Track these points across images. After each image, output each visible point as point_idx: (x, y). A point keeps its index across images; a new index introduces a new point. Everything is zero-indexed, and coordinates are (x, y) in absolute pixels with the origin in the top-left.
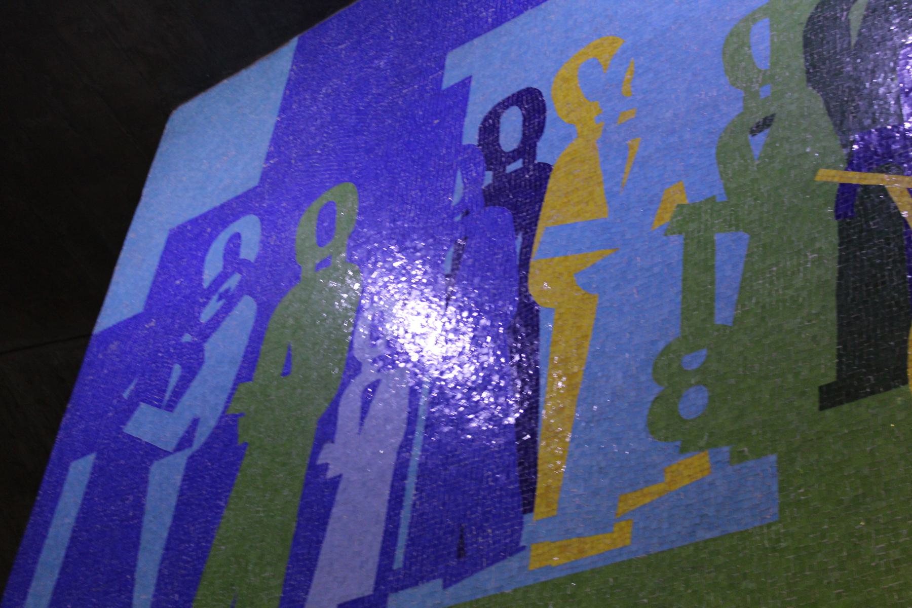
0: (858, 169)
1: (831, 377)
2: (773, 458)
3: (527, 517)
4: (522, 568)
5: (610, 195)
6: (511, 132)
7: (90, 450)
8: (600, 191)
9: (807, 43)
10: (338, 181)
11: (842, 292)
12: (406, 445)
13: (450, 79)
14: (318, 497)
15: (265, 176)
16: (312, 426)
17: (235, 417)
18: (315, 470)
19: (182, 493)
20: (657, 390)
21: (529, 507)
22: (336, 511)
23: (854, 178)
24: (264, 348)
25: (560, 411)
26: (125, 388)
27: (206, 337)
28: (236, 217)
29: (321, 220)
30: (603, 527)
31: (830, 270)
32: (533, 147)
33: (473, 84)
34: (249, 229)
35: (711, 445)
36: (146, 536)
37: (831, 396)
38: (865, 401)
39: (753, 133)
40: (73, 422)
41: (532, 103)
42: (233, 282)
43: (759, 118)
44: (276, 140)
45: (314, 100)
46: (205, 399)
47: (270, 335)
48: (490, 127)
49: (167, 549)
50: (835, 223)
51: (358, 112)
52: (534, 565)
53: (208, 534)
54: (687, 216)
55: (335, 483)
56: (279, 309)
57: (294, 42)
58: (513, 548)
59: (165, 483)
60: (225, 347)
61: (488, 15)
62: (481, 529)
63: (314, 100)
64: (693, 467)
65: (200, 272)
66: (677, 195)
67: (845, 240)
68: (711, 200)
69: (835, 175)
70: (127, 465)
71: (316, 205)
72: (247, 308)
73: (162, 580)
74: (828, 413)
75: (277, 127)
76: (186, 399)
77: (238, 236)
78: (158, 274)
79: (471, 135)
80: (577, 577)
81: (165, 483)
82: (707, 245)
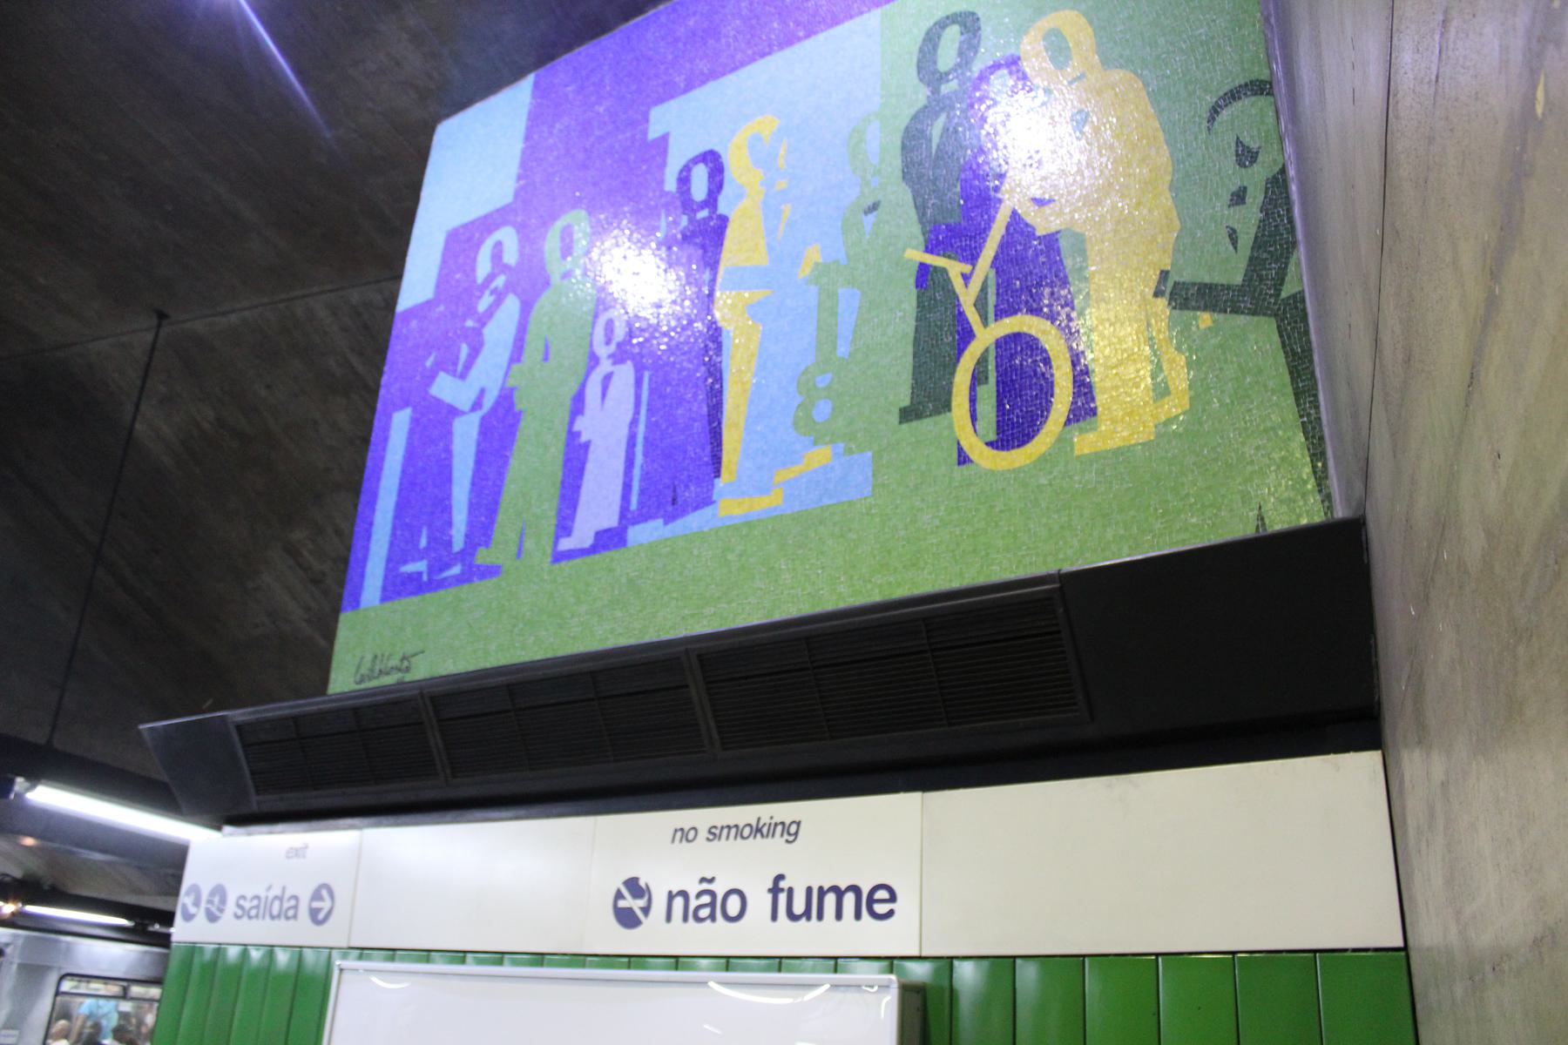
0: (931, 252)
1: (906, 402)
2: (870, 454)
4: (714, 515)
5: (770, 248)
6: (699, 190)
7: (406, 404)
8: (762, 242)
9: (904, 147)
10: (574, 207)
11: (916, 342)
12: (634, 422)
13: (654, 133)
14: (576, 456)
15: (517, 194)
16: (568, 403)
17: (512, 390)
18: (572, 435)
19: (479, 444)
22: (589, 466)
26: (426, 357)
27: (484, 324)
28: (498, 227)
29: (563, 239)
30: (765, 491)
32: (716, 200)
33: (671, 141)
34: (508, 237)
35: (831, 442)
36: (456, 474)
37: (907, 415)
38: (926, 421)
39: (866, 213)
40: (391, 382)
41: (713, 161)
42: (500, 281)
43: (870, 202)
44: (524, 164)
45: (550, 133)
46: (489, 372)
47: (532, 328)
48: (684, 180)
49: (473, 484)
50: (914, 291)
51: (586, 150)
52: (722, 513)
53: (501, 475)
54: (821, 270)
55: (586, 446)
56: (537, 306)
57: (530, 80)
58: (706, 501)
59: (465, 437)
60: (499, 332)
61: (680, 80)
62: (687, 487)
63: (550, 133)
64: (821, 456)
65: (473, 270)
67: (920, 305)
69: (918, 255)
70: (434, 422)
71: (559, 224)
72: (512, 304)
73: (473, 508)
74: (905, 426)
75: (524, 152)
76: (474, 372)
77: (499, 245)
78: (441, 269)
79: (671, 185)
80: (749, 524)
81: (465, 437)
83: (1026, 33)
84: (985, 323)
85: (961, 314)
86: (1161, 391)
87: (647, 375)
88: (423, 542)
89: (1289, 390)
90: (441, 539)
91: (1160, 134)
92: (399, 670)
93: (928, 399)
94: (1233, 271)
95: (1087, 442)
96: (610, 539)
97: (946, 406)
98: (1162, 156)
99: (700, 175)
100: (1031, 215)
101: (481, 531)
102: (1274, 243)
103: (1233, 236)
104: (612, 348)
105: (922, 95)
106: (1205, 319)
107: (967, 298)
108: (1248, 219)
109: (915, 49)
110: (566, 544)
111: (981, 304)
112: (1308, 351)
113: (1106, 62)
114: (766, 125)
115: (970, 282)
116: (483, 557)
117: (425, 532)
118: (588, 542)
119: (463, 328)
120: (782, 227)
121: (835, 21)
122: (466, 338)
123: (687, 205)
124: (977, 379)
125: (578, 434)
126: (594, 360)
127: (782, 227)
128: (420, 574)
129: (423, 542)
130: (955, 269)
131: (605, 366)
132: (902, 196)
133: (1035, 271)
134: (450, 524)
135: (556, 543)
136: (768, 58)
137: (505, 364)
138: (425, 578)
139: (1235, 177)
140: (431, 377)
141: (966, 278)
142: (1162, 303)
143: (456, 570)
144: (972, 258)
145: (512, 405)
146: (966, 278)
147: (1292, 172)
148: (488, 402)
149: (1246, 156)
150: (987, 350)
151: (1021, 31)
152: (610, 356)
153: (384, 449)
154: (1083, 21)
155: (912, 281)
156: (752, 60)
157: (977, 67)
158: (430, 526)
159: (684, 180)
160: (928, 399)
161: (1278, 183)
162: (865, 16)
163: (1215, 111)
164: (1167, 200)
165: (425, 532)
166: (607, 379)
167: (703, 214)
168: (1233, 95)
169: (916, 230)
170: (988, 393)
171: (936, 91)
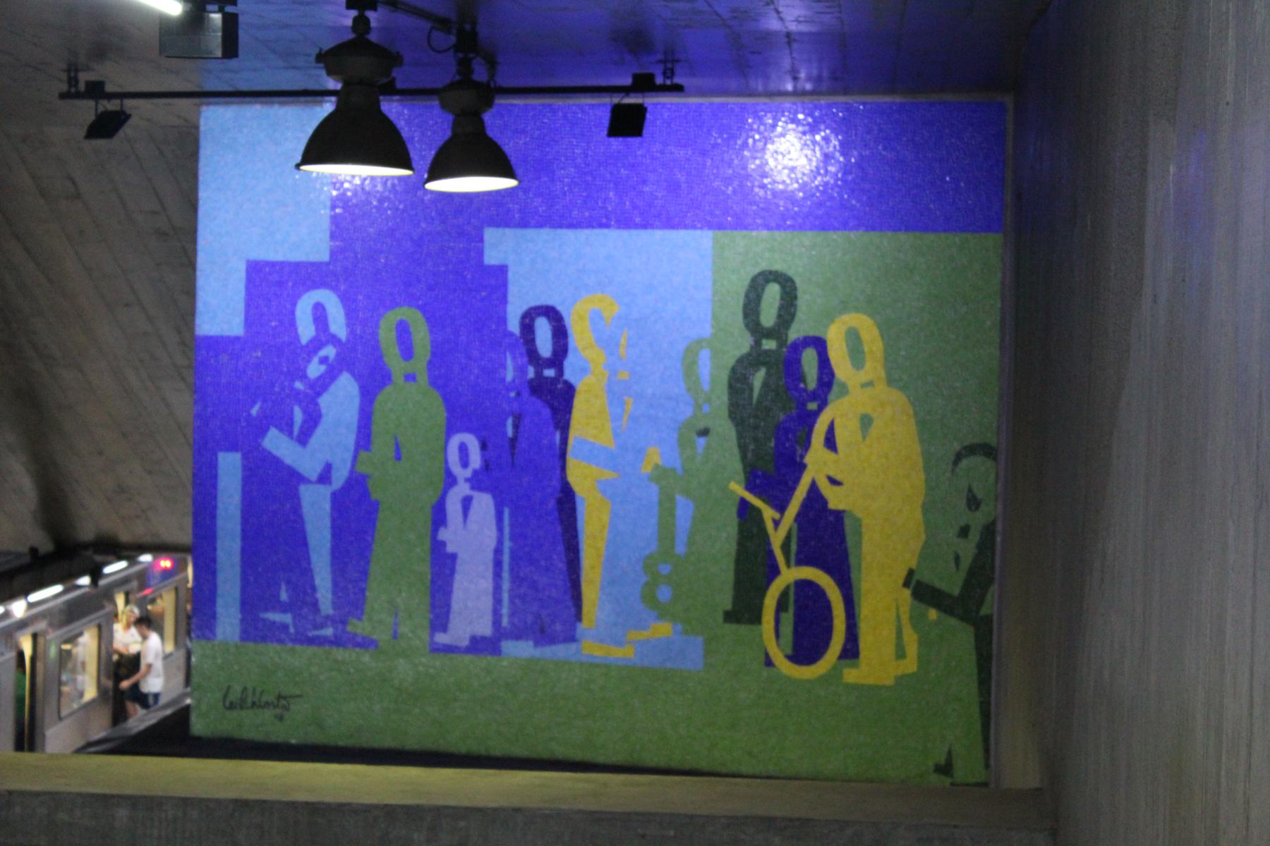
1: (729, 607)
3: (578, 624)
5: (616, 435)
6: (545, 345)
7: (233, 447)
8: (609, 425)
12: (498, 551)
13: (492, 257)
14: (443, 564)
16: (428, 511)
19: (333, 521)
20: (644, 579)
21: (578, 617)
24: (374, 428)
25: (593, 568)
27: (319, 394)
30: (620, 643)
31: (732, 547)
37: (730, 617)
42: (330, 351)
43: (702, 425)
47: (377, 418)
52: (585, 652)
54: (661, 474)
55: (453, 557)
56: (380, 398)
59: (316, 507)
64: (663, 629)
65: (293, 324)
66: (654, 457)
67: (741, 531)
68: (674, 470)
79: (514, 326)
82: (671, 499)
83: (832, 321)
84: (788, 566)
85: (771, 553)
86: (900, 653)
87: (507, 512)
88: (284, 596)
89: (975, 677)
90: (304, 597)
91: (920, 459)
92: (276, 707)
93: (745, 610)
94: (952, 584)
95: (851, 675)
97: (756, 619)
98: (919, 478)
99: (543, 329)
100: (826, 490)
103: (957, 559)
104: (468, 473)
105: (743, 343)
106: (933, 614)
107: (777, 539)
108: (968, 549)
109: (742, 292)
110: (441, 638)
111: (786, 546)
112: (990, 657)
113: (890, 381)
114: (610, 308)
115: (780, 527)
117: (283, 587)
118: (465, 643)
119: (292, 389)
120: (626, 417)
121: (670, 223)
122: (300, 402)
123: (533, 355)
124: (781, 606)
125: (443, 544)
126: (451, 480)
127: (626, 417)
128: (285, 627)
129: (284, 596)
130: (768, 513)
131: (462, 489)
132: (726, 430)
133: (825, 536)
134: (314, 589)
135: (432, 636)
136: (605, 231)
137: (352, 448)
138: (292, 630)
140: (263, 431)
141: (777, 523)
142: (907, 593)
143: (329, 632)
144: (781, 508)
145: (365, 494)
146: (777, 523)
147: (999, 527)
149: (973, 503)
150: (788, 587)
151: (830, 317)
152: (467, 480)
153: (215, 486)
154: (876, 332)
155: (734, 510)
156: (590, 226)
157: (794, 334)
158: (288, 582)
160: (745, 610)
161: (989, 530)
162: (698, 232)
163: (958, 457)
164: (918, 515)
165: (283, 587)
166: (467, 503)
167: (550, 373)
168: (971, 450)
169: (738, 466)
170: (788, 618)
171: (758, 343)
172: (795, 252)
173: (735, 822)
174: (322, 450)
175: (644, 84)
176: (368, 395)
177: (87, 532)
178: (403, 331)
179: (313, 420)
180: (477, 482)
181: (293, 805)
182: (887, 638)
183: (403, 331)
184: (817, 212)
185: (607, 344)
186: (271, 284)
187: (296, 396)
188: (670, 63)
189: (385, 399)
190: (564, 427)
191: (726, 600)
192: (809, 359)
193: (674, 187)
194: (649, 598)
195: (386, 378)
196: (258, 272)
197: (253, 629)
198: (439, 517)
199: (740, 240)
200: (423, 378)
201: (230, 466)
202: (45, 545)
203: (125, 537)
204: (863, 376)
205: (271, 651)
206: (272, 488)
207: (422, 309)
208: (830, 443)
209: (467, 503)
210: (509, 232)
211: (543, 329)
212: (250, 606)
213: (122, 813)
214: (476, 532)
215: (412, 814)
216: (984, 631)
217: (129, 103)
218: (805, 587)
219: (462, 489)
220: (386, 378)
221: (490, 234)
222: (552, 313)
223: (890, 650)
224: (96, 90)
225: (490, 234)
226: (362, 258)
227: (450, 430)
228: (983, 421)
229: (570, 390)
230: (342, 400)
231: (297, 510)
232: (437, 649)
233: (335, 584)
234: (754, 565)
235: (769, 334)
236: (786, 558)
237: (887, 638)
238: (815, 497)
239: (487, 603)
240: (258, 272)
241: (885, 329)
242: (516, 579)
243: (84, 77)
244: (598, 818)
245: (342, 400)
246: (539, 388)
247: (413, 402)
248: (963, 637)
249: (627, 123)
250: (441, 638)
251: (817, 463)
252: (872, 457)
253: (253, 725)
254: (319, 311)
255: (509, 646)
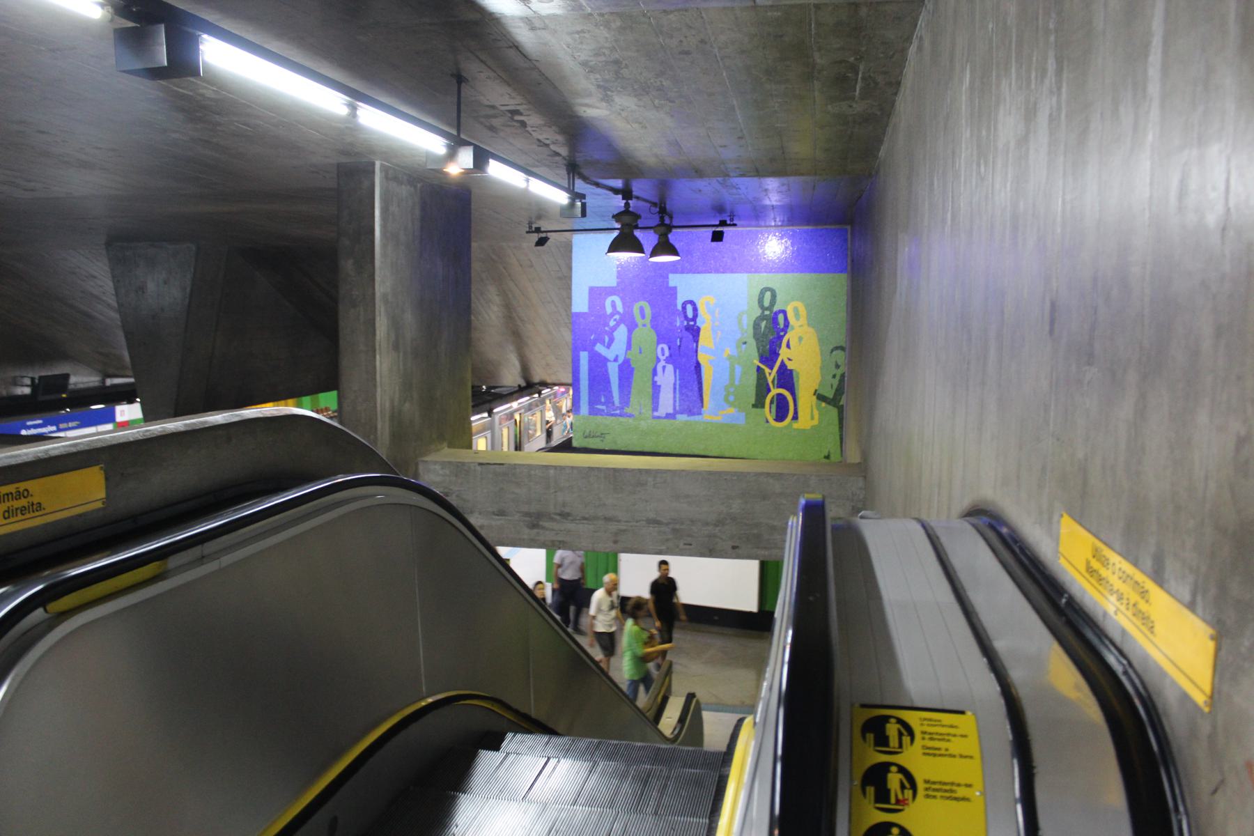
6: (690, 314)
13: (671, 284)
18: (654, 383)
23: (762, 366)
37: (754, 406)
42: (617, 317)
48: (684, 308)
54: (730, 357)
59: (613, 370)
64: (732, 410)
65: (604, 307)
66: (728, 351)
79: (679, 307)
86: (812, 418)
93: (759, 404)
94: (830, 394)
95: (796, 425)
96: (668, 416)
97: (763, 406)
99: (689, 308)
100: (787, 362)
101: (625, 400)
102: (839, 391)
105: (758, 312)
106: (823, 404)
107: (770, 379)
108: (836, 382)
110: (656, 414)
114: (712, 301)
115: (771, 375)
116: (628, 410)
121: (732, 272)
123: (686, 317)
124: (772, 402)
126: (658, 360)
130: (767, 370)
131: (662, 363)
132: (752, 343)
133: (786, 378)
139: (834, 371)
140: (595, 344)
148: (621, 360)
149: (837, 366)
151: (787, 303)
157: (776, 309)
159: (684, 308)
160: (759, 404)
161: (843, 376)
164: (819, 371)
166: (664, 368)
168: (837, 348)
169: (757, 354)
170: (774, 407)
172: (775, 280)
173: (758, 474)
174: (614, 351)
175: (723, 223)
176: (630, 331)
177: (536, 379)
178: (642, 309)
179: (612, 340)
180: (668, 361)
181: (608, 469)
182: (808, 412)
183: (642, 309)
184: (784, 267)
185: (712, 313)
186: (597, 294)
187: (606, 332)
188: (732, 217)
189: (636, 332)
190: (697, 342)
191: (753, 401)
192: (781, 318)
193: (734, 259)
194: (727, 400)
195: (636, 326)
196: (593, 291)
197: (593, 411)
198: (655, 372)
199: (756, 276)
200: (649, 326)
201: (584, 357)
202: (523, 384)
203: (549, 381)
204: (799, 323)
205: (599, 418)
206: (598, 363)
207: (649, 302)
208: (788, 346)
209: (664, 368)
210: (678, 275)
211: (689, 308)
212: (592, 403)
213: (552, 472)
214: (668, 377)
215: (648, 472)
216: (841, 411)
217: (549, 234)
218: (779, 395)
219: (662, 363)
220: (636, 326)
221: (671, 276)
222: (692, 302)
223: (809, 417)
224: (538, 230)
225: (671, 276)
226: (626, 286)
227: (658, 343)
228: (841, 338)
229: (698, 330)
230: (621, 333)
231: (606, 371)
232: (655, 418)
233: (620, 397)
234: (762, 389)
235: (767, 309)
236: (775, 388)
237: (808, 412)
238: (783, 364)
239: (671, 402)
240: (593, 291)
241: (807, 306)
242: (681, 393)
243: (534, 226)
244: (710, 473)
245: (621, 333)
246: (688, 328)
247: (645, 334)
248: (834, 412)
249: (717, 237)
250: (656, 414)
251: (784, 353)
252: (804, 353)
253: (592, 444)
254: (613, 303)
255: (679, 416)
